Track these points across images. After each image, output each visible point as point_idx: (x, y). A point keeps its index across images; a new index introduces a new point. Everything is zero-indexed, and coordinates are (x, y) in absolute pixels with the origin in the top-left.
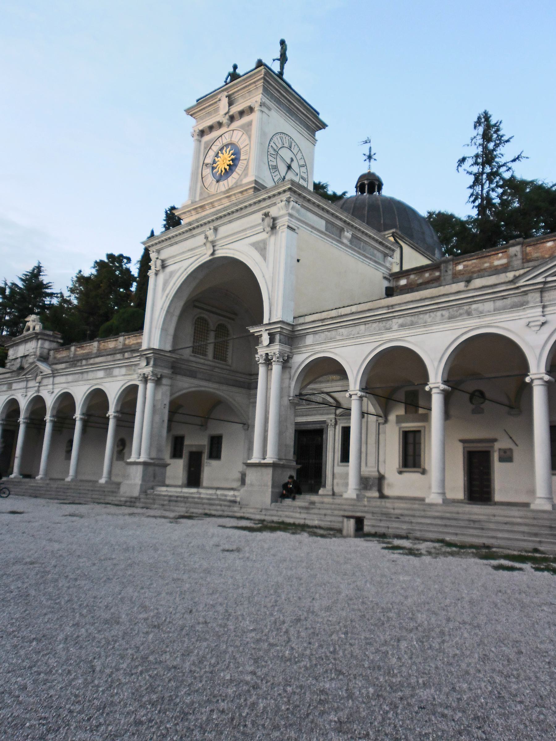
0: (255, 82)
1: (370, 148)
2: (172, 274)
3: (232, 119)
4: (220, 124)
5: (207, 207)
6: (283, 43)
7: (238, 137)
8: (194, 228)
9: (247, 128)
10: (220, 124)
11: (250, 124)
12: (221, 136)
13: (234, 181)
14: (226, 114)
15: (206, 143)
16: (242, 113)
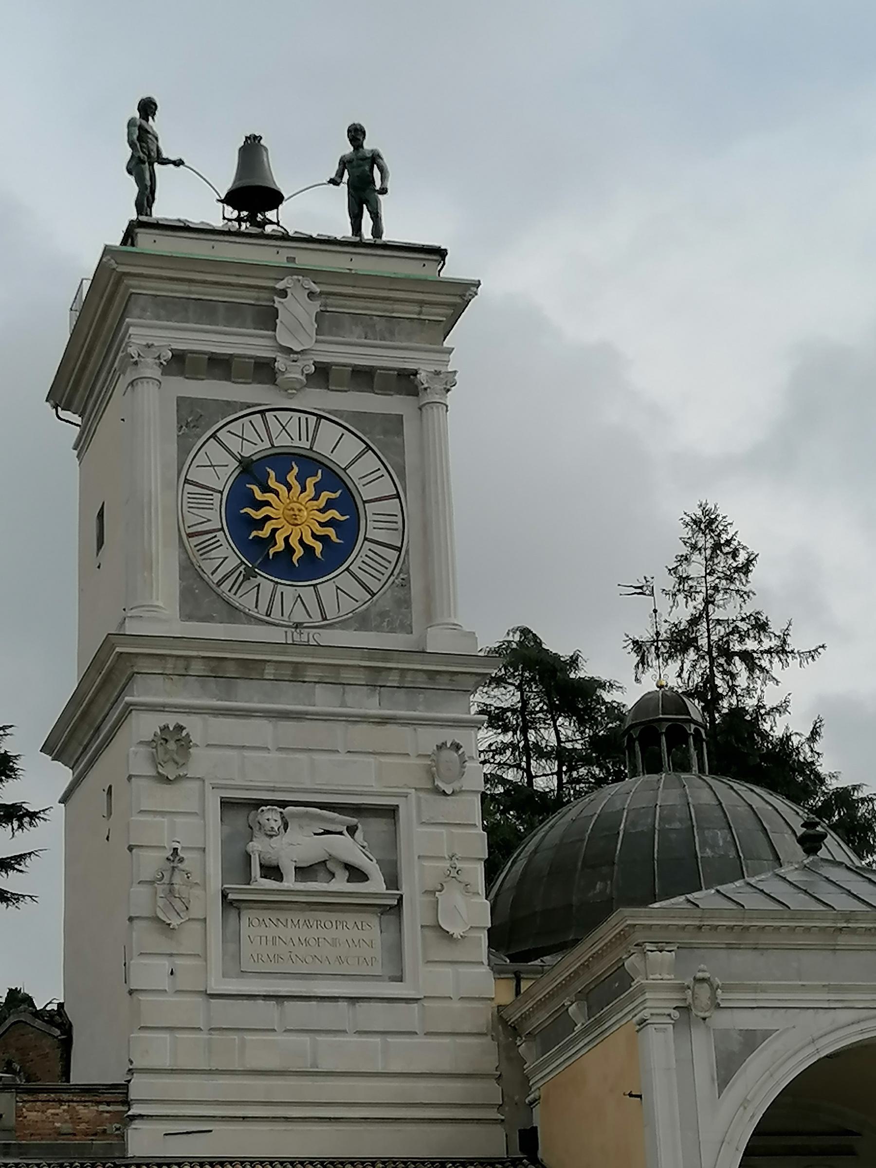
0: (422, 303)
1: (655, 611)
2: (752, 1040)
3: (323, 375)
4: (264, 371)
5: (269, 672)
6: (356, 134)
7: (338, 448)
8: (854, 931)
9: (383, 436)
10: (264, 371)
11: (394, 425)
12: (262, 412)
13: (348, 605)
14: (303, 352)
15: (181, 401)
16: (364, 378)
